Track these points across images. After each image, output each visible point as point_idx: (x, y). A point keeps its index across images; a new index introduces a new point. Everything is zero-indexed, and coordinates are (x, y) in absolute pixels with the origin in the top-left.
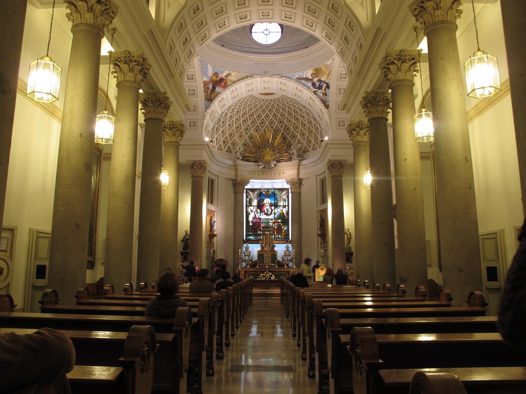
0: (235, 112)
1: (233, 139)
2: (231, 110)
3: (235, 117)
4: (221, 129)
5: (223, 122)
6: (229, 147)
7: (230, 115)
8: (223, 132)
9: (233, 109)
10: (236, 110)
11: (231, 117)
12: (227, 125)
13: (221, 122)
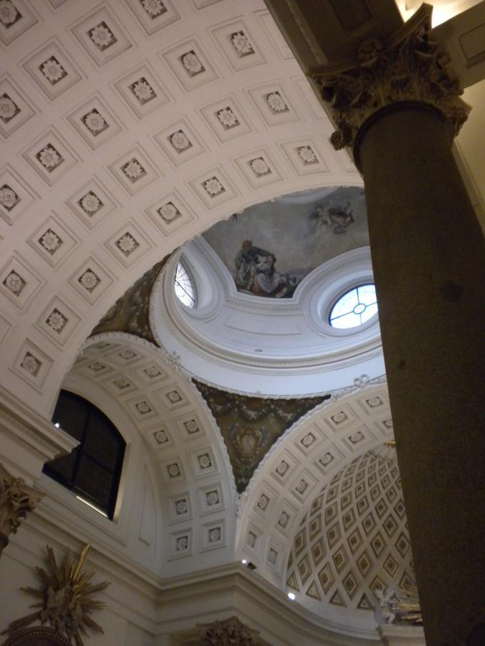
6: (364, 597)
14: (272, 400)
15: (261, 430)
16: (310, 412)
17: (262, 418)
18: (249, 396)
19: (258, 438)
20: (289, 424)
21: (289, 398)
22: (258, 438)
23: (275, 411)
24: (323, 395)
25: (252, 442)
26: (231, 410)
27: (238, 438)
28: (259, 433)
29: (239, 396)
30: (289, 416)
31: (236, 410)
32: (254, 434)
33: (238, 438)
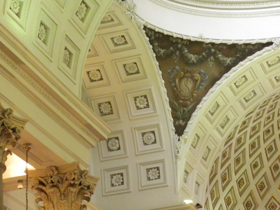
0: (261, 134)
1: (268, 197)
2: (249, 129)
3: (264, 146)
4: (235, 178)
5: (237, 161)
7: (249, 142)
8: (240, 183)
9: (254, 129)
10: (263, 129)
11: (253, 146)
12: (247, 167)
13: (232, 161)
14: (213, 44)
15: (200, 73)
16: (250, 57)
17: (201, 61)
18: (193, 39)
19: (197, 81)
20: (228, 68)
21: (230, 43)
22: (197, 81)
23: (214, 54)
24: (265, 42)
25: (190, 85)
26: (172, 53)
27: (177, 81)
28: (197, 76)
29: (182, 39)
30: (228, 60)
31: (178, 53)
32: (192, 78)
33: (177, 81)
